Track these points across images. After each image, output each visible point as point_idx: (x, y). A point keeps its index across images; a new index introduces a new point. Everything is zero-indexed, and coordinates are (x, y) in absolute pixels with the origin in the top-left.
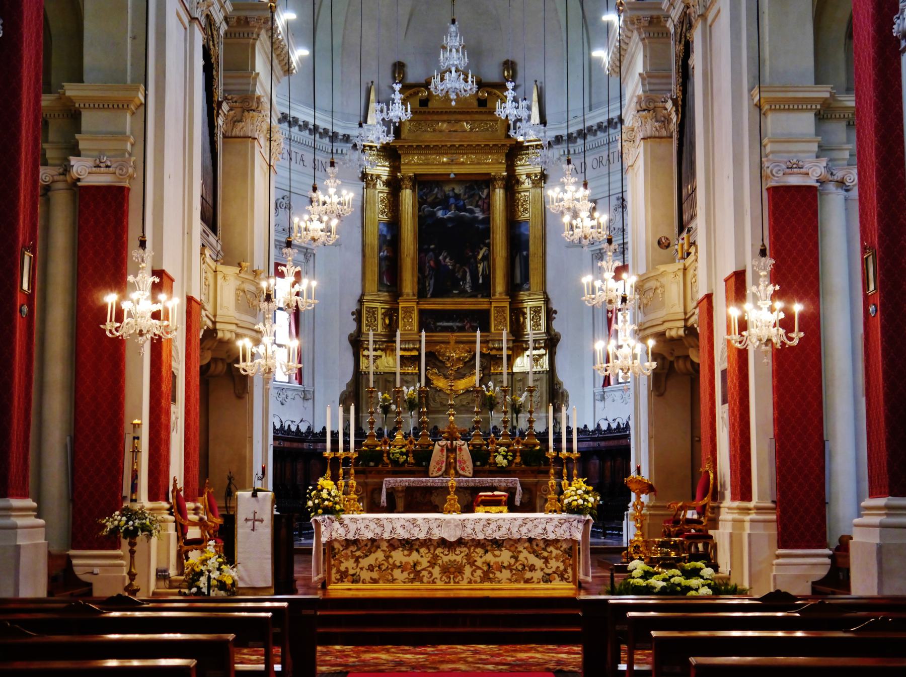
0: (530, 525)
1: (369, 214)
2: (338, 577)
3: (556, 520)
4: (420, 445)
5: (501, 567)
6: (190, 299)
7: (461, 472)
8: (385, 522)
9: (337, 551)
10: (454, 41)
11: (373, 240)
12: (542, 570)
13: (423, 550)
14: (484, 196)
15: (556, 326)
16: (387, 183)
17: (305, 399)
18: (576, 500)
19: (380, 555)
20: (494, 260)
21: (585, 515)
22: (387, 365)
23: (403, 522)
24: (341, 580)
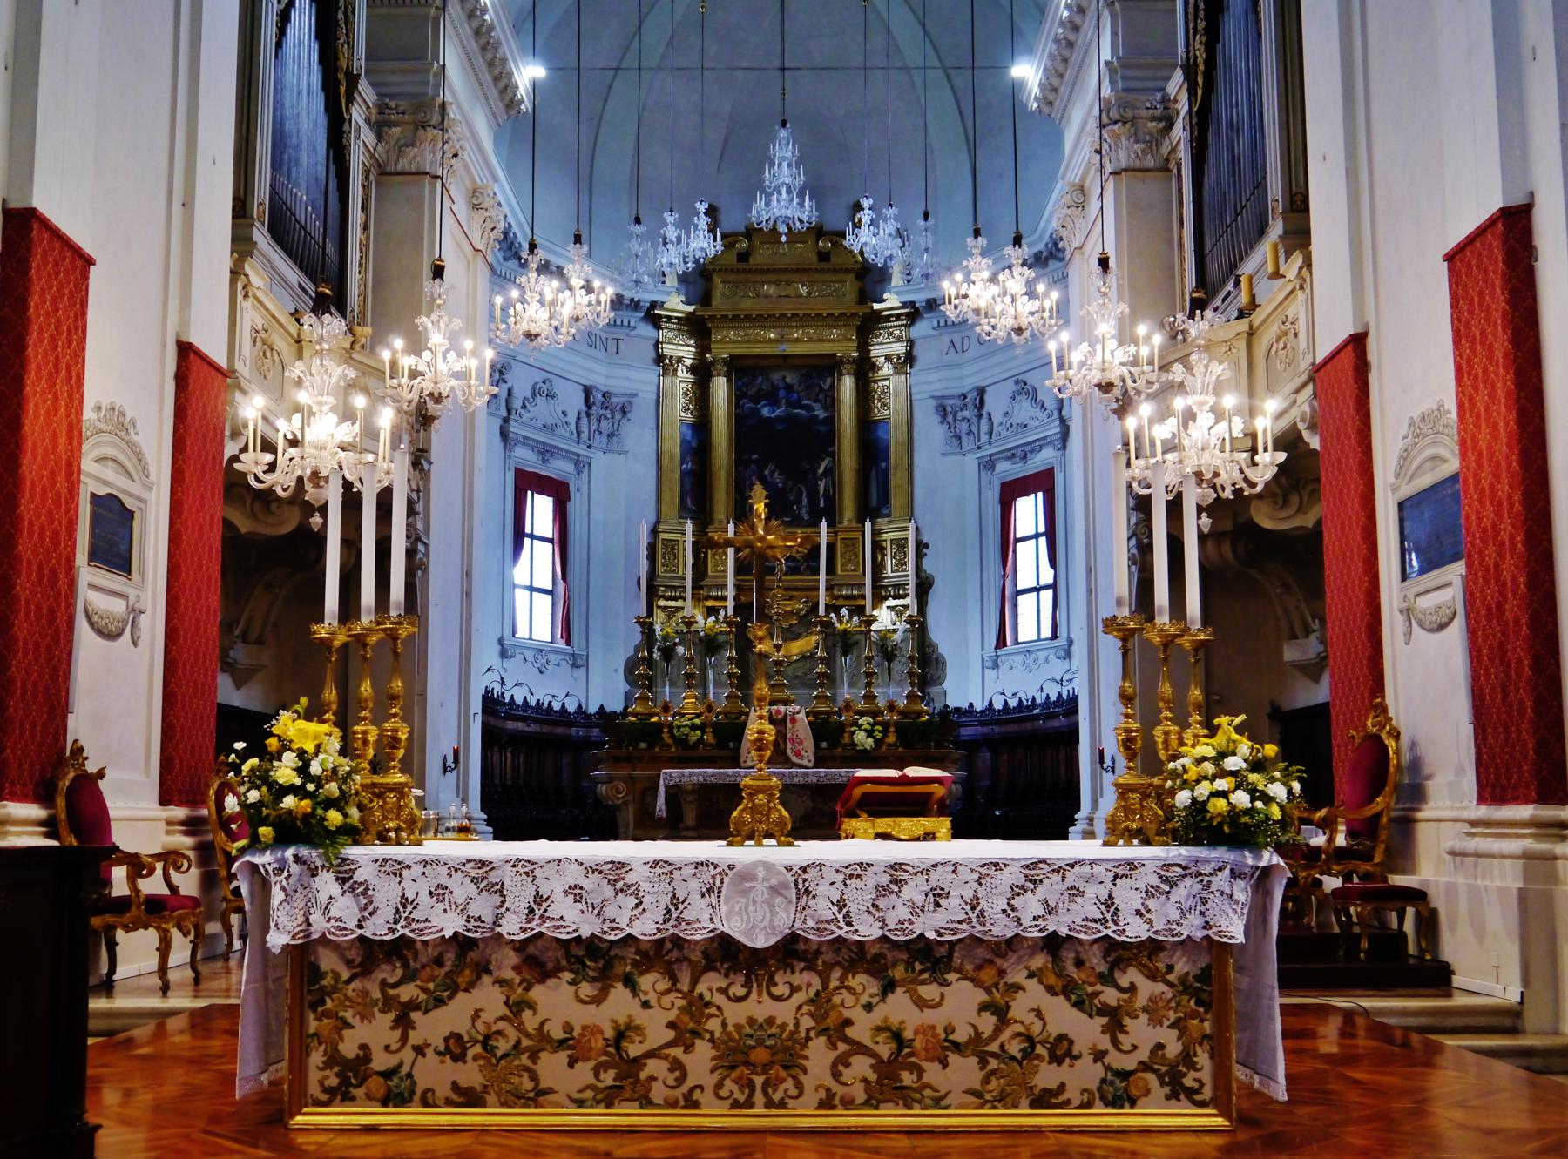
0: (1051, 888)
1: (665, 412)
2: (333, 1081)
3: (1151, 867)
4: (726, 715)
5: (946, 1047)
6: (185, 350)
7: (795, 759)
8: (508, 876)
9: (328, 981)
10: (784, 150)
11: (673, 446)
12: (1099, 1056)
13: (650, 982)
14: (826, 387)
15: (928, 565)
16: (692, 369)
17: (575, 666)
18: (1224, 794)
19: (488, 999)
20: (841, 476)
21: (1256, 849)
23: (574, 875)
24: (340, 1094)
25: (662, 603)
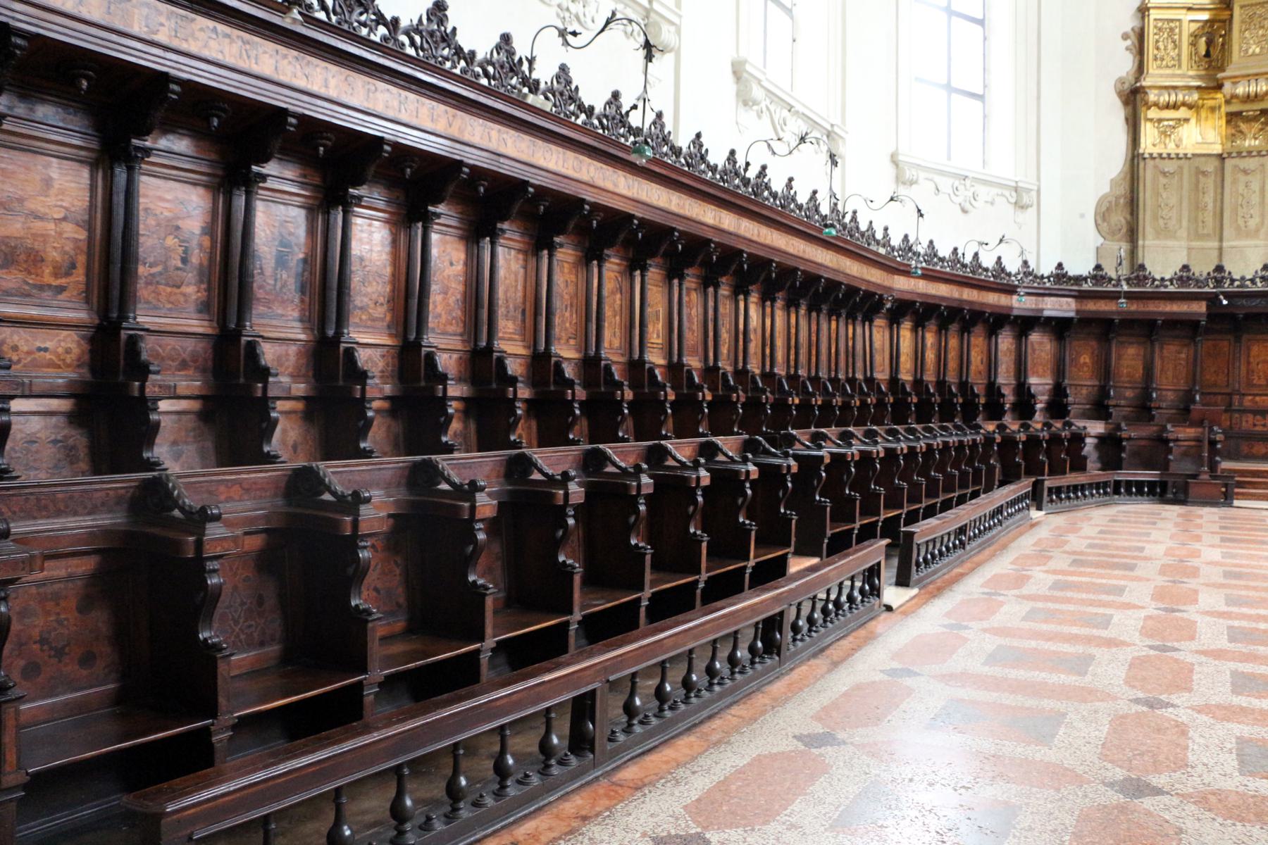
17: (1020, 206)
22: (1200, 140)
25: (1153, 113)
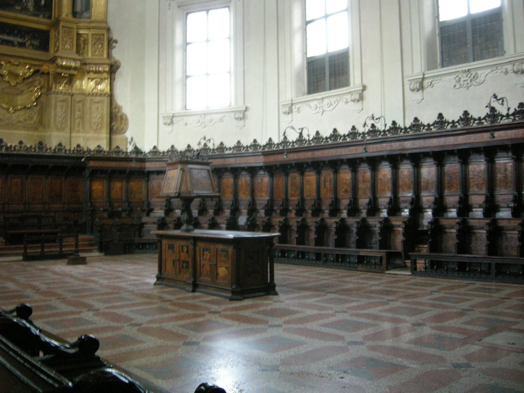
15: (116, 54)
